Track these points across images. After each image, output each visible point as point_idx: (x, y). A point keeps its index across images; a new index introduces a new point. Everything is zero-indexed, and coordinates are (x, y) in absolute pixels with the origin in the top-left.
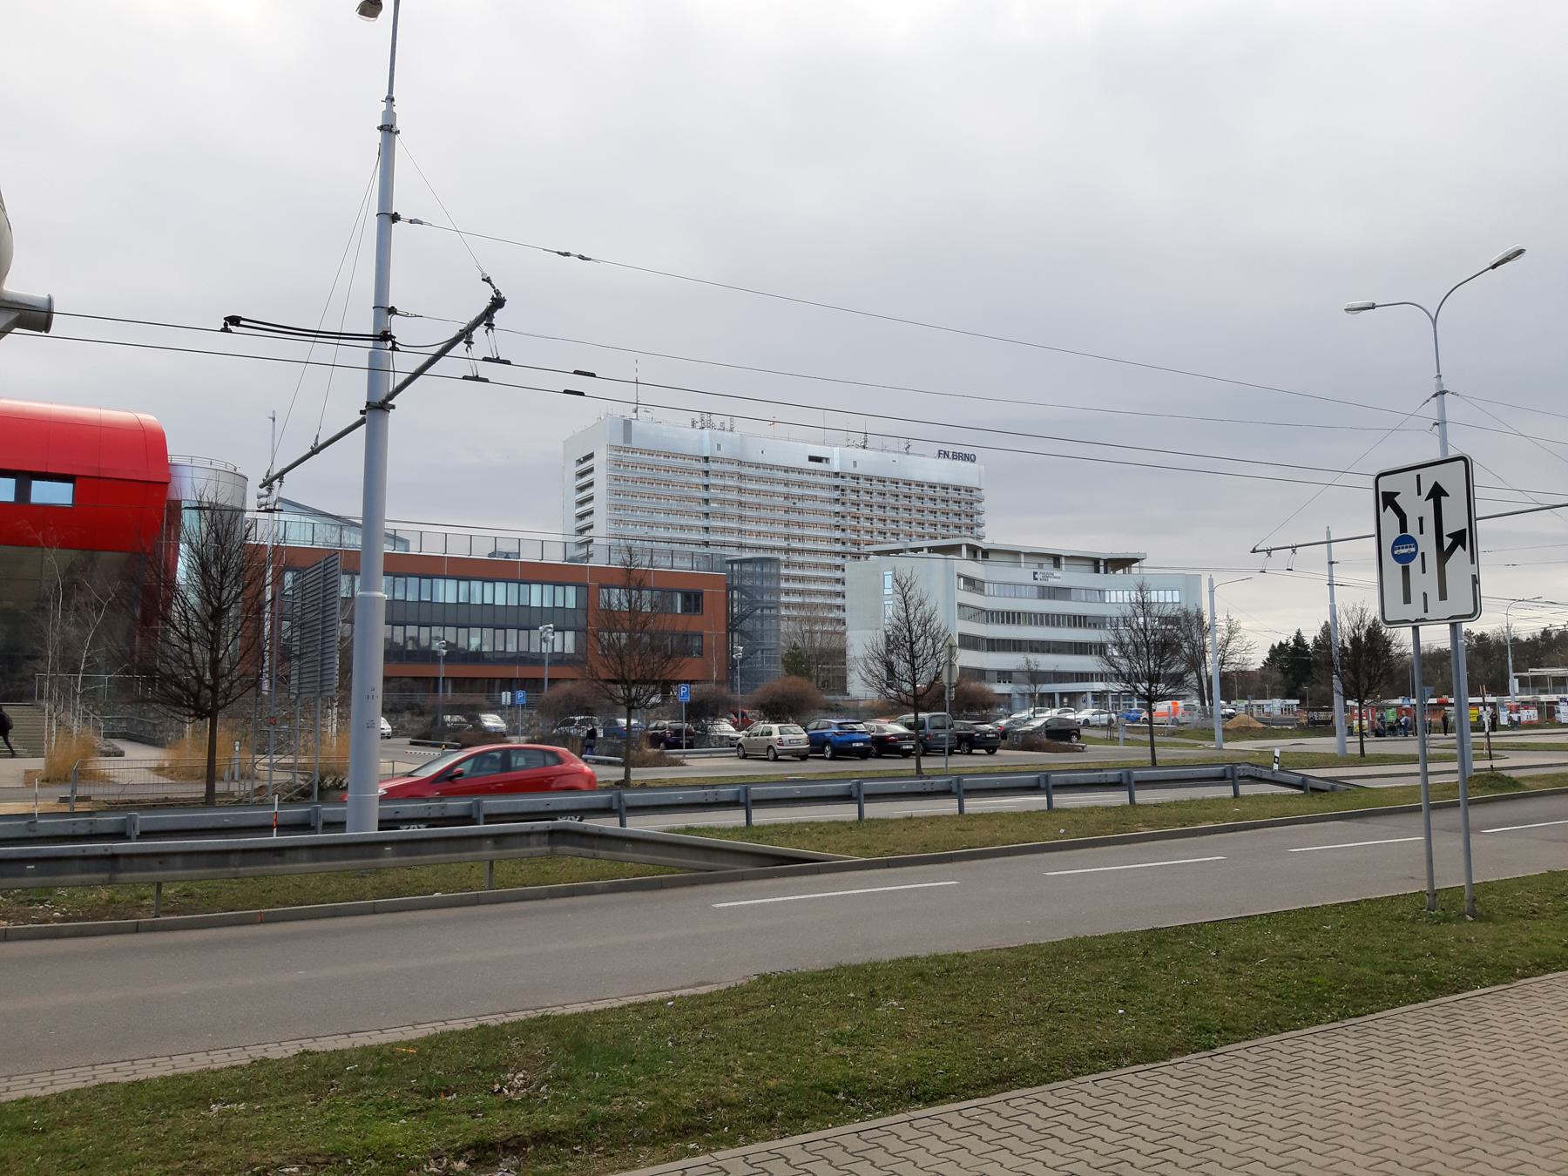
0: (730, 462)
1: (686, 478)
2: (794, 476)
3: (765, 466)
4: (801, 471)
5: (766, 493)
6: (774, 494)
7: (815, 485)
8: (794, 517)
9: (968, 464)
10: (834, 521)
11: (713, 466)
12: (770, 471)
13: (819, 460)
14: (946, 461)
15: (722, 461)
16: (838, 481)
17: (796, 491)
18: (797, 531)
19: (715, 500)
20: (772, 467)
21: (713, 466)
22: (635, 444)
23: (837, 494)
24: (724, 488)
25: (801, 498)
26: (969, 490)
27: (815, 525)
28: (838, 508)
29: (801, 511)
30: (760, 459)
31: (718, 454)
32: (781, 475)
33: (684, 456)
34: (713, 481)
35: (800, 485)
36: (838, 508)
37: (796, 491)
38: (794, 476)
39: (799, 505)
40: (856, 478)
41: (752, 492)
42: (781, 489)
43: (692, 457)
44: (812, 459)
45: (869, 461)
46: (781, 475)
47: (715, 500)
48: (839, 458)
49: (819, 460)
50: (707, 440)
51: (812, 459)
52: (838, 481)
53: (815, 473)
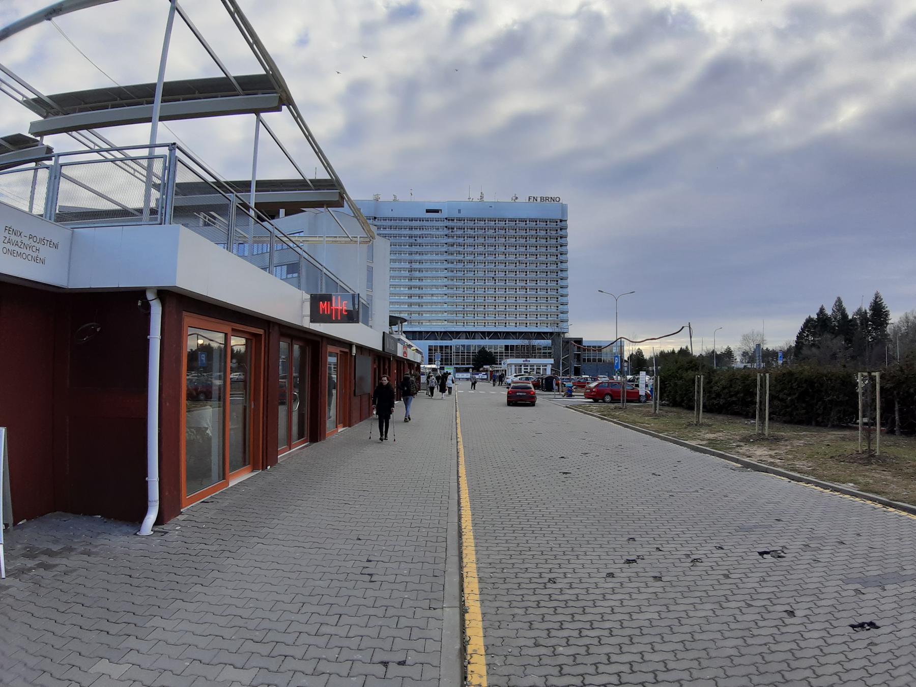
2: (418, 223)
3: (395, 219)
4: (421, 220)
6: (400, 236)
7: (432, 227)
8: (414, 249)
10: (445, 248)
13: (437, 211)
16: (450, 224)
17: (418, 232)
18: (418, 257)
20: (401, 219)
25: (421, 236)
27: (431, 253)
32: (408, 223)
35: (421, 228)
37: (418, 232)
38: (418, 223)
39: (419, 240)
40: (459, 220)
42: (407, 232)
44: (428, 211)
46: (408, 223)
49: (437, 211)
51: (428, 211)
52: (450, 224)
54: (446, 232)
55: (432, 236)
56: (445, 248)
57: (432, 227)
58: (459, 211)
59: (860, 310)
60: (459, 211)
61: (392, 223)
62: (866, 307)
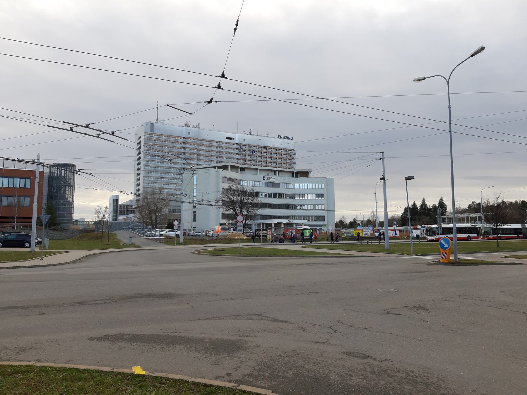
0: (194, 139)
1: (176, 145)
2: (220, 145)
3: (208, 141)
4: (222, 143)
5: (209, 151)
6: (211, 151)
7: (229, 148)
8: (219, 159)
9: (290, 141)
11: (187, 140)
12: (210, 143)
13: (230, 139)
14: (281, 140)
15: (191, 138)
16: (238, 147)
19: (187, 153)
20: (211, 141)
21: (187, 140)
22: (155, 132)
23: (237, 151)
24: (191, 149)
26: (290, 150)
28: (237, 156)
29: (222, 158)
30: (206, 138)
31: (189, 136)
32: (215, 144)
33: (175, 137)
34: (187, 146)
36: (237, 156)
38: (220, 145)
39: (222, 155)
41: (203, 150)
42: (215, 149)
43: (178, 137)
45: (249, 140)
47: (187, 153)
48: (238, 138)
49: (230, 139)
50: (184, 131)
51: (227, 138)
52: (238, 147)
53: (228, 143)
54: (237, 151)
55: (228, 153)
56: (236, 161)
57: (229, 148)
58: (244, 140)
59: (434, 205)
60: (244, 140)
61: (207, 143)
62: (437, 203)
